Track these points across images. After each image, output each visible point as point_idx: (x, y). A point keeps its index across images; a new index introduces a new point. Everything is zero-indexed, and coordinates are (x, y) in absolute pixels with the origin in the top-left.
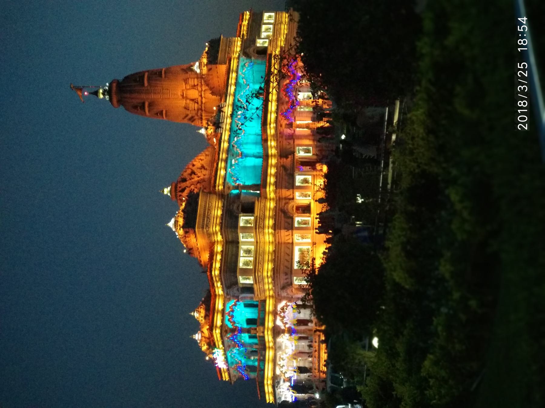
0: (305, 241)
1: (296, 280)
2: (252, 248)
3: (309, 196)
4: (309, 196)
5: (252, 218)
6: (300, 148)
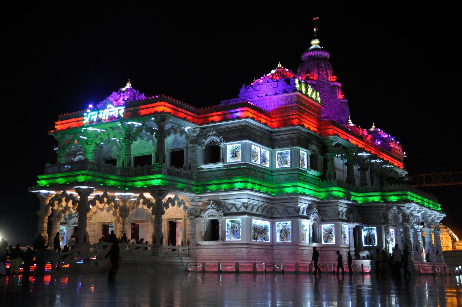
0: (278, 234)
1: (232, 221)
2: (268, 165)
3: (326, 242)
4: (326, 242)
5: (306, 167)
6: (375, 232)
